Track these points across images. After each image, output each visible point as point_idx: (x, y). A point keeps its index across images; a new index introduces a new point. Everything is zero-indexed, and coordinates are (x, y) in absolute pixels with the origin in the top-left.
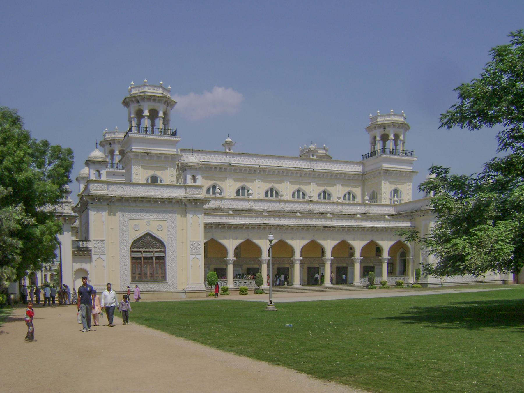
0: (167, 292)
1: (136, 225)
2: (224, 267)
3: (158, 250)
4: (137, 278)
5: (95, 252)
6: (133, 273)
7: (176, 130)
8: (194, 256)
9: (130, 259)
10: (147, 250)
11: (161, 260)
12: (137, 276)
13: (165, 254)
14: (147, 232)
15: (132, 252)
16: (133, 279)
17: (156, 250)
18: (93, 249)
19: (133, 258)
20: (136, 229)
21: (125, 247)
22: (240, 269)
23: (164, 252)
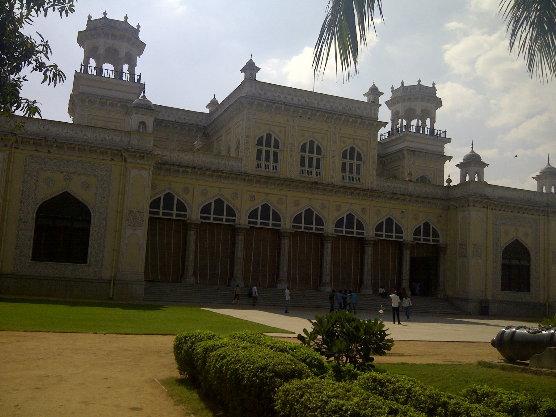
7: (140, 76)
11: (84, 234)
16: (37, 256)
23: (89, 221)
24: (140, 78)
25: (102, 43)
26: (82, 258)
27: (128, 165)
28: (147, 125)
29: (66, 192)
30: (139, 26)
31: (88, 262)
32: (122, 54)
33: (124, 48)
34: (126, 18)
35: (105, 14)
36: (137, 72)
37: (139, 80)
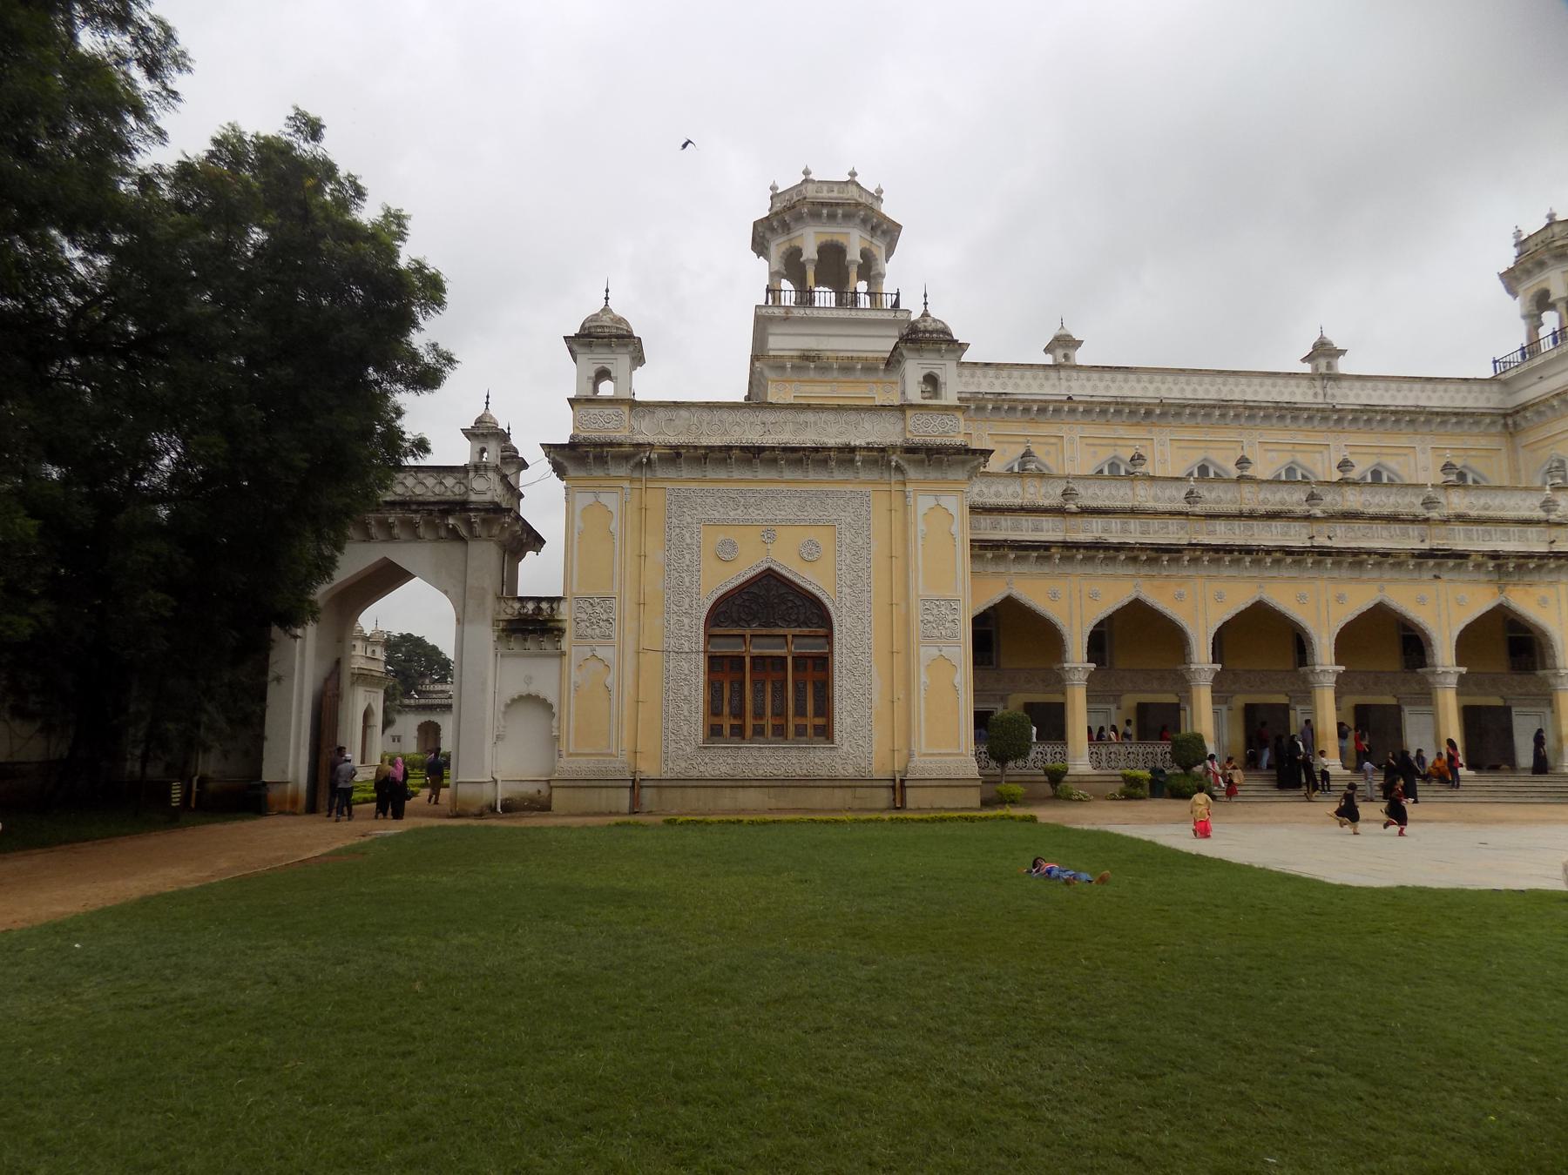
0: (834, 783)
1: (723, 543)
2: (1057, 698)
3: (805, 630)
4: (727, 730)
5: (579, 637)
6: (714, 708)
8: (934, 652)
9: (701, 661)
10: (764, 631)
11: (818, 669)
12: (727, 723)
13: (831, 644)
14: (765, 566)
15: (710, 637)
16: (714, 732)
17: (797, 631)
18: (569, 626)
19: (715, 663)
20: (727, 557)
21: (686, 621)
22: (1113, 707)
23: (829, 637)
24: (897, 300)
25: (810, 241)
26: (825, 732)
27: (909, 488)
28: (941, 380)
29: (769, 569)
30: (880, 191)
31: (837, 738)
32: (854, 255)
33: (855, 242)
34: (853, 174)
35: (806, 172)
36: (888, 286)
37: (896, 305)
